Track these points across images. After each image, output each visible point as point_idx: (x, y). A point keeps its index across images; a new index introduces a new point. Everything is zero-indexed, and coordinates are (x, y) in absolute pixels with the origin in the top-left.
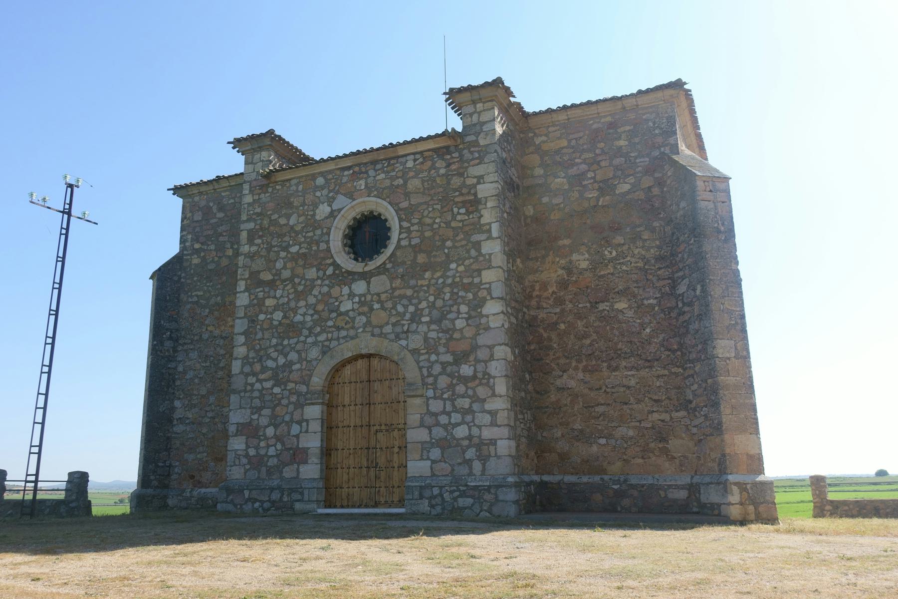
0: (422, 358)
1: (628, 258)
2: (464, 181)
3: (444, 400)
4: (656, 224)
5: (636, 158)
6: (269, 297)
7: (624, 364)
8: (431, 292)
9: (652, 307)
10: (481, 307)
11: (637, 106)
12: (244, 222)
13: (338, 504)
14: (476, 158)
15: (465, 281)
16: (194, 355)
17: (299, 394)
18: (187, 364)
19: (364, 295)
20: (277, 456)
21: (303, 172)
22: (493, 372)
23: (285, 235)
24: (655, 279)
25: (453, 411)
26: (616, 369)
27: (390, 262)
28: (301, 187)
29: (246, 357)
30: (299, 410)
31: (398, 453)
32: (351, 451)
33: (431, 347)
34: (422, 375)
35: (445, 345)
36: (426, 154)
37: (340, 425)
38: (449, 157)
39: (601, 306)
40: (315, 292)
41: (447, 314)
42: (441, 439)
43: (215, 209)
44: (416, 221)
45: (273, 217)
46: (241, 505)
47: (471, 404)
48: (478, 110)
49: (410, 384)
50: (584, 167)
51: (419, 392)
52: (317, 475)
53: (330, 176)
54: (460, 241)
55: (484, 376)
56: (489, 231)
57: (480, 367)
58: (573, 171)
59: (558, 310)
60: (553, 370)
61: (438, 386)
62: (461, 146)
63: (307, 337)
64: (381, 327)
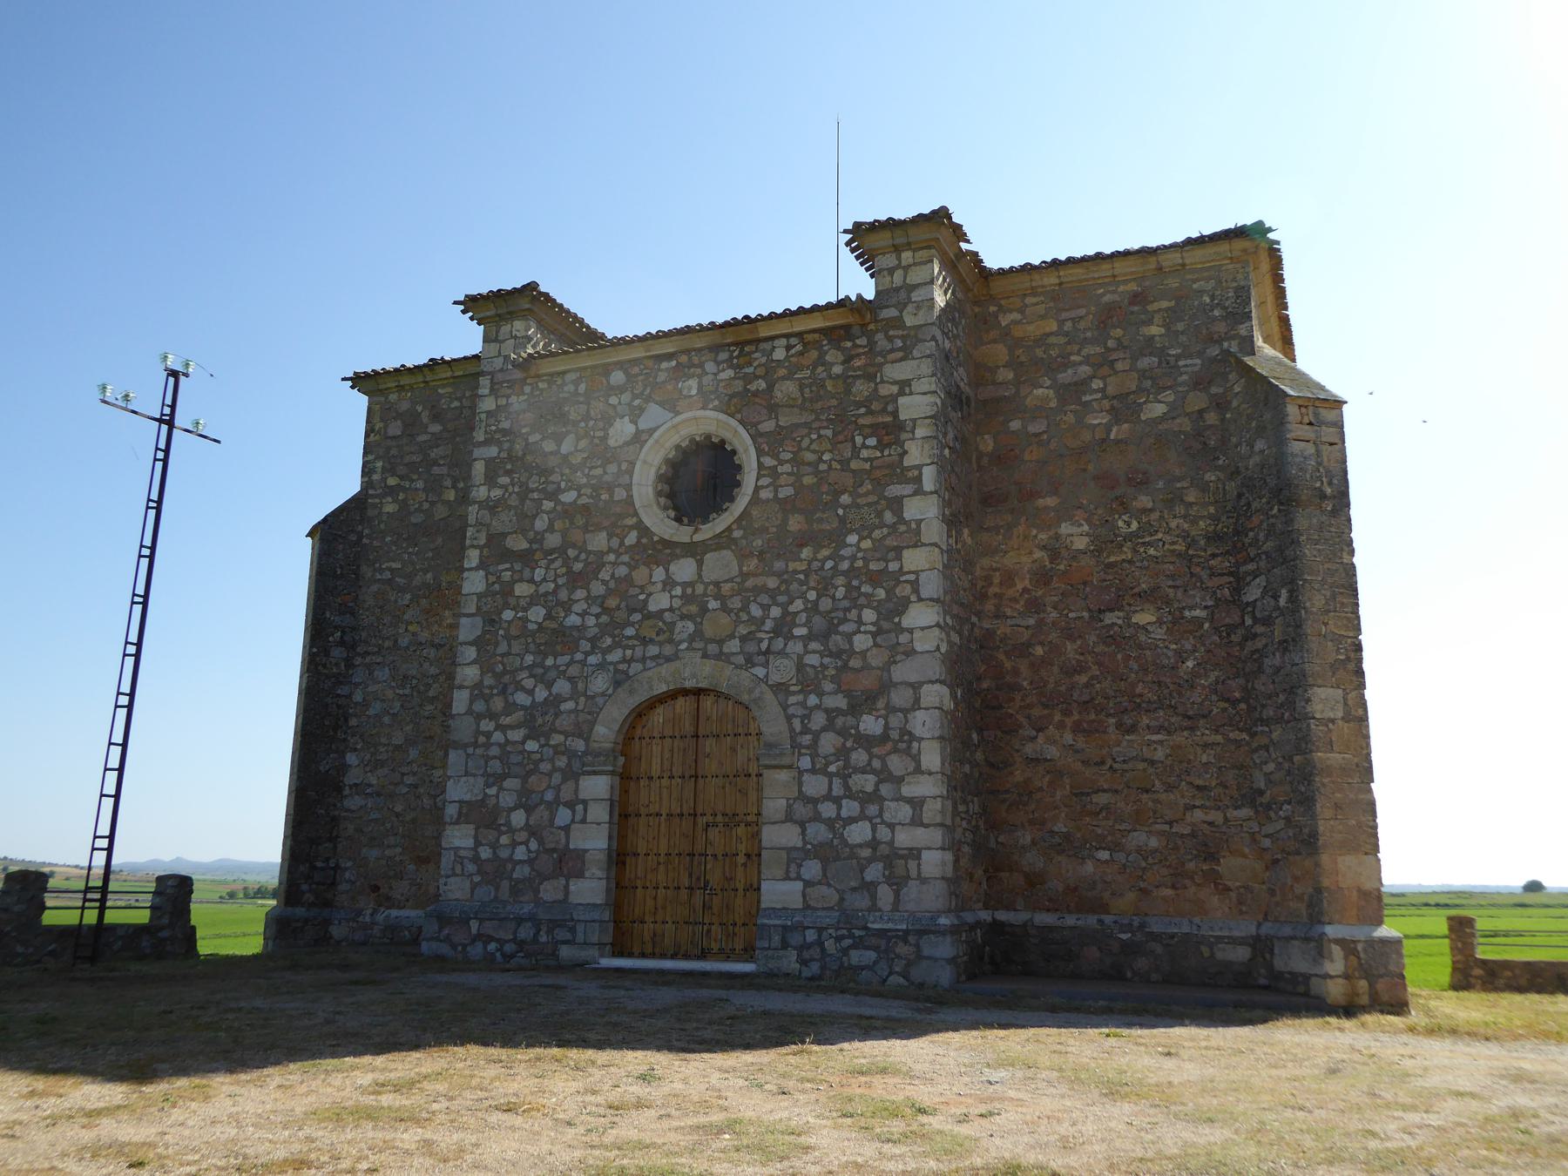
0: (792, 699)
1: (1160, 536)
2: (876, 390)
3: (830, 776)
4: (1210, 477)
5: (1178, 358)
6: (521, 580)
7: (1145, 721)
8: (812, 584)
9: (1198, 622)
10: (901, 614)
11: (1183, 265)
12: (481, 444)
13: (636, 951)
14: (900, 349)
15: (873, 566)
16: (383, 674)
17: (571, 754)
18: (370, 689)
19: (691, 584)
20: (530, 862)
21: (586, 361)
22: (918, 731)
24: (1204, 575)
25: (846, 797)
26: (1132, 729)
29: (478, 685)
30: (570, 784)
31: (745, 865)
32: (662, 859)
33: (809, 682)
34: (792, 730)
35: (833, 679)
36: (809, 337)
37: (643, 811)
38: (849, 344)
39: (1109, 618)
41: (839, 624)
42: (821, 845)
43: (425, 418)
45: (532, 439)
46: (465, 946)
47: (877, 785)
48: (904, 263)
49: (770, 746)
50: (1085, 370)
51: (786, 761)
52: (599, 899)
53: (636, 370)
54: (866, 494)
55: (902, 736)
56: (918, 480)
57: (896, 721)
58: (1066, 377)
59: (1032, 622)
60: (1021, 726)
61: (820, 751)
62: (872, 327)
63: (587, 654)
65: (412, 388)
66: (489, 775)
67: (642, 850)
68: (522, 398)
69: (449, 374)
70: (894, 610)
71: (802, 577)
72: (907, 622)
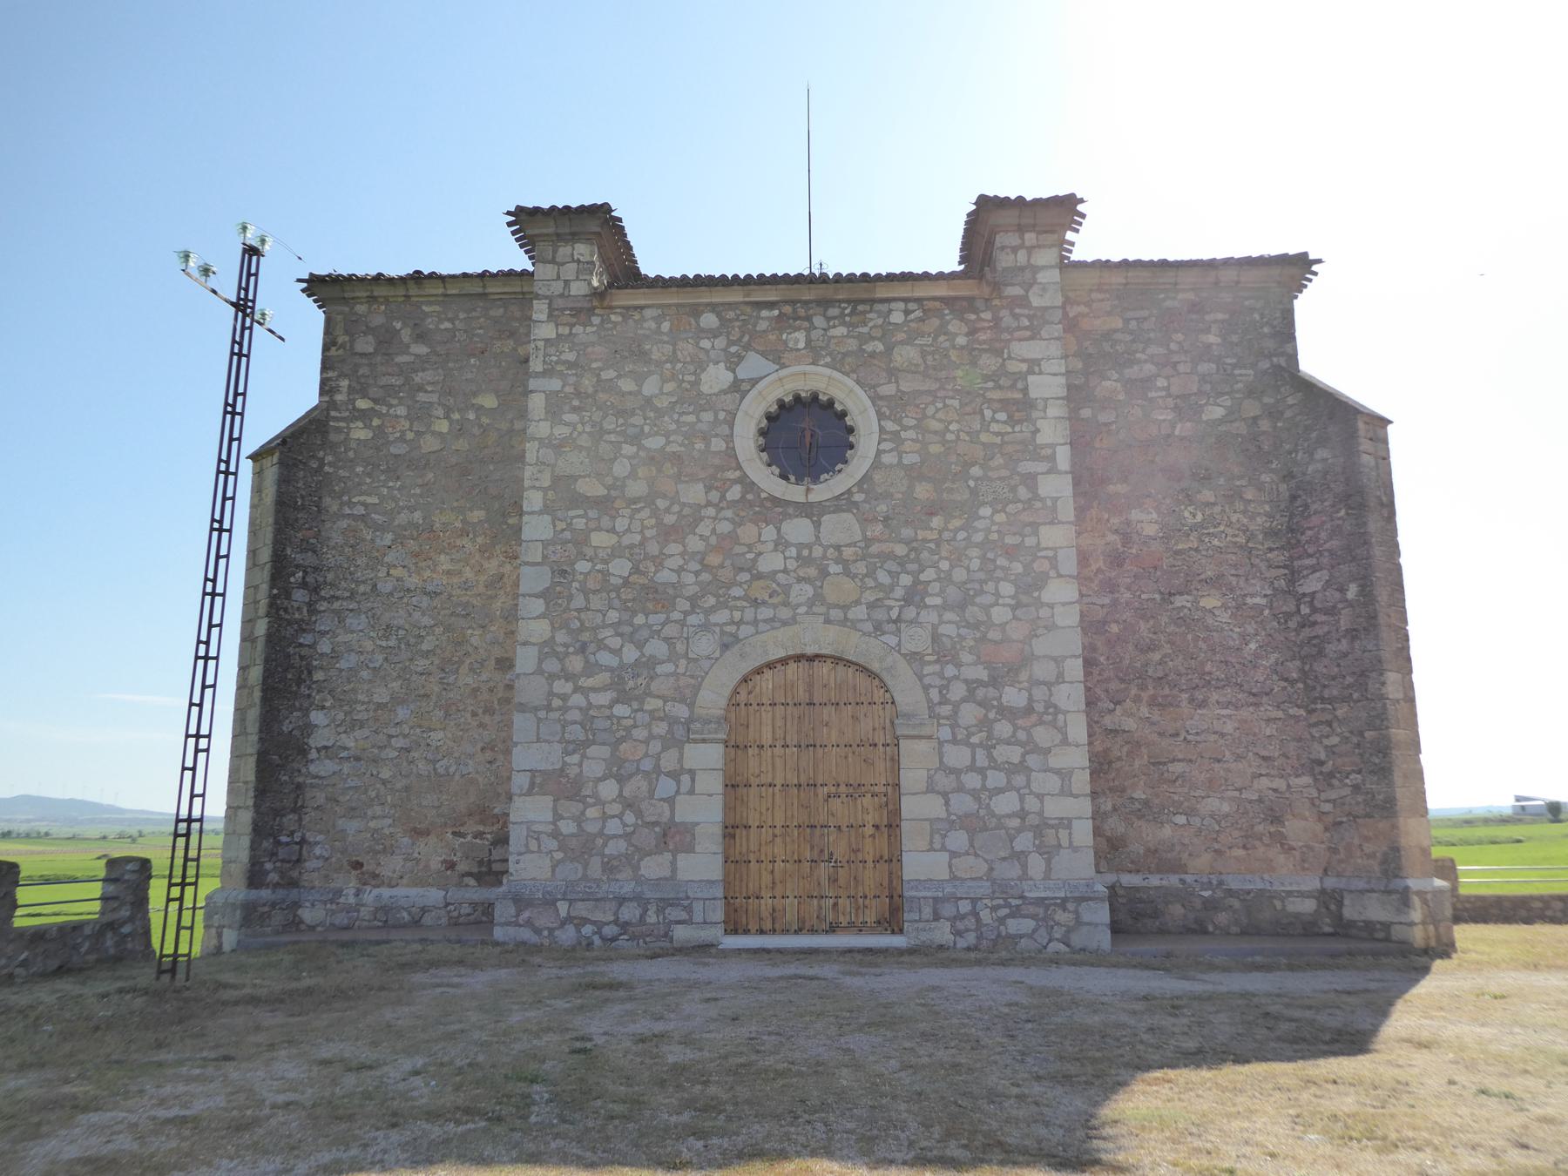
0: (928, 670)
2: (1003, 365)
3: (973, 747)
4: (1266, 478)
5: (1234, 366)
6: (599, 529)
7: (1215, 696)
8: (944, 554)
10: (1040, 589)
12: (537, 375)
13: (753, 927)
14: (1026, 328)
15: (1009, 540)
16: (358, 622)
17: (673, 721)
18: (339, 639)
19: (809, 546)
20: (627, 836)
22: (1063, 704)
23: (633, 414)
24: (1263, 566)
26: (1203, 704)
27: (861, 491)
28: (666, 326)
29: (550, 642)
30: (673, 754)
31: (873, 836)
32: (777, 831)
34: (929, 700)
37: (753, 780)
38: (973, 317)
39: (1179, 601)
40: (704, 529)
41: (976, 595)
42: (967, 816)
43: (406, 335)
44: (913, 422)
45: (605, 375)
46: (551, 930)
47: (1023, 756)
48: (1027, 244)
50: (1149, 368)
51: (926, 731)
53: (731, 315)
55: (1047, 708)
56: (1052, 458)
57: (1039, 693)
58: (1132, 372)
59: (1107, 601)
60: (1099, 699)
61: (960, 722)
63: (686, 613)
64: (845, 608)
65: (387, 300)
66: (568, 742)
67: (754, 823)
68: (589, 329)
69: (440, 291)
70: (1032, 585)
71: (932, 546)
72: (1046, 596)
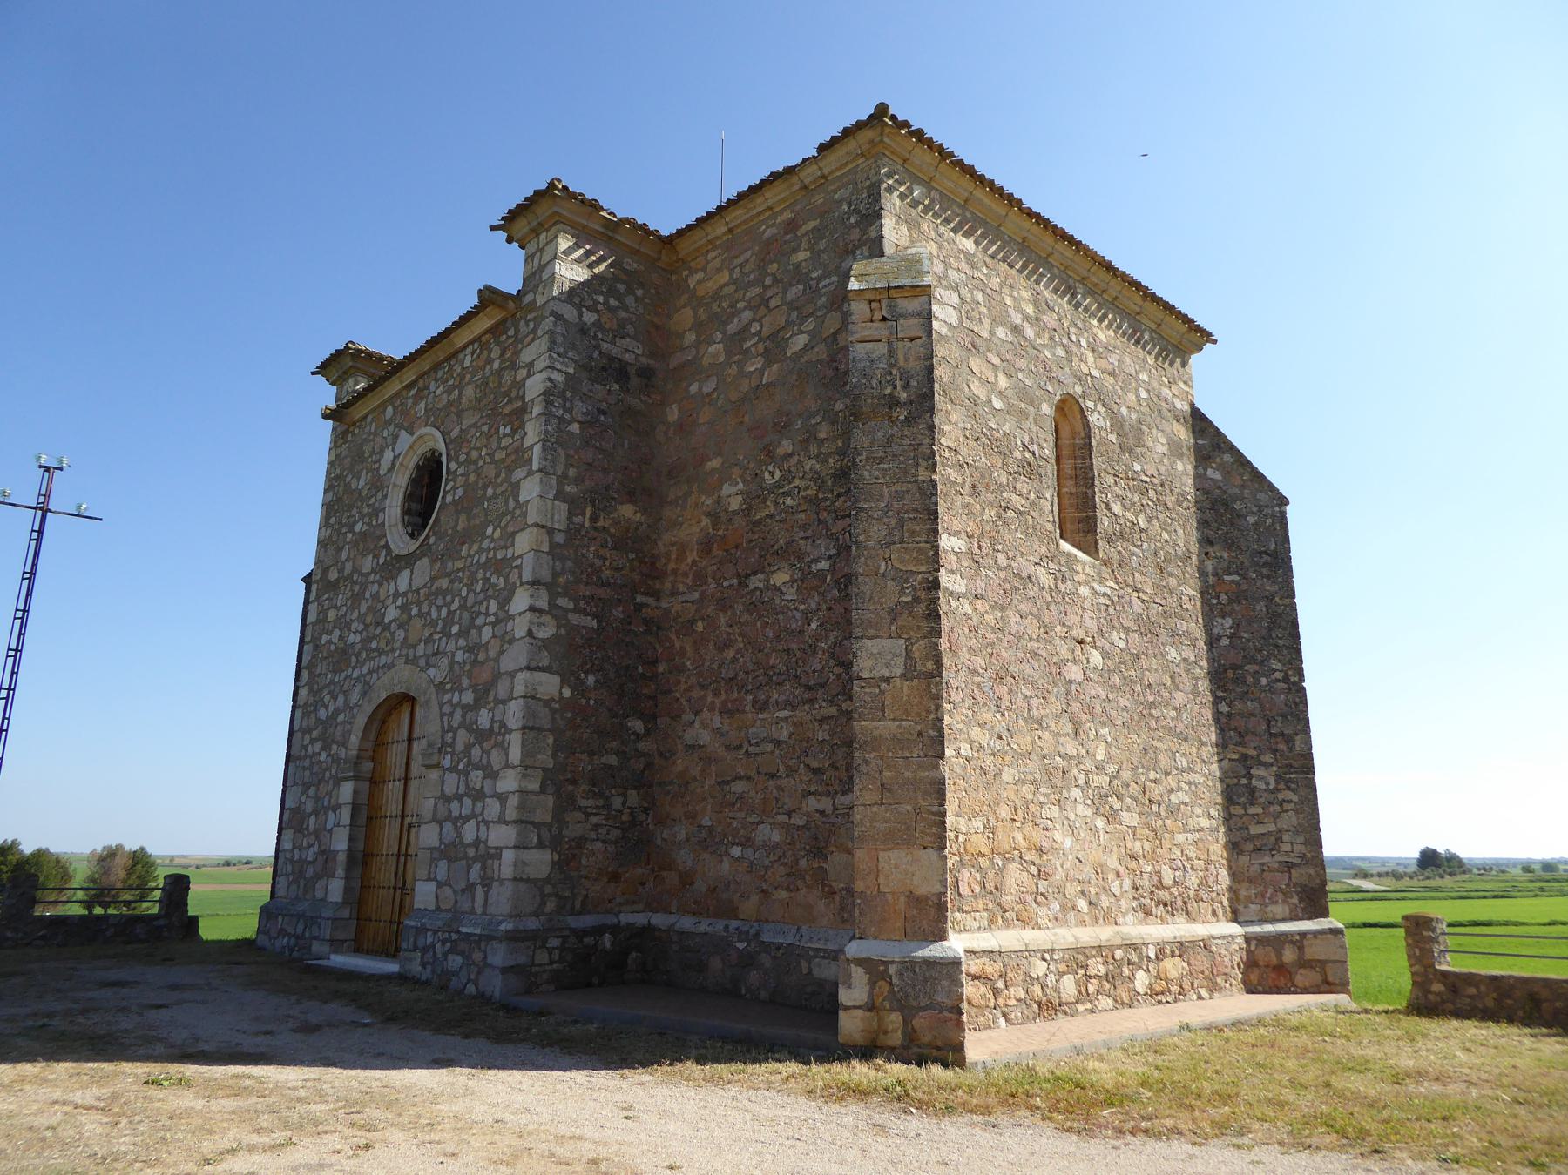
1: (797, 482)
5: (819, 280)
9: (821, 574)
11: (824, 177)
50: (748, 314)
